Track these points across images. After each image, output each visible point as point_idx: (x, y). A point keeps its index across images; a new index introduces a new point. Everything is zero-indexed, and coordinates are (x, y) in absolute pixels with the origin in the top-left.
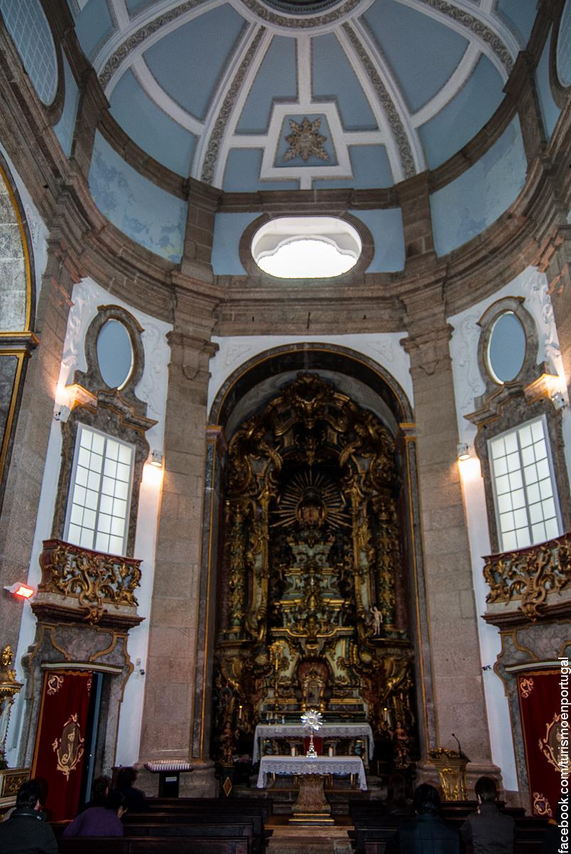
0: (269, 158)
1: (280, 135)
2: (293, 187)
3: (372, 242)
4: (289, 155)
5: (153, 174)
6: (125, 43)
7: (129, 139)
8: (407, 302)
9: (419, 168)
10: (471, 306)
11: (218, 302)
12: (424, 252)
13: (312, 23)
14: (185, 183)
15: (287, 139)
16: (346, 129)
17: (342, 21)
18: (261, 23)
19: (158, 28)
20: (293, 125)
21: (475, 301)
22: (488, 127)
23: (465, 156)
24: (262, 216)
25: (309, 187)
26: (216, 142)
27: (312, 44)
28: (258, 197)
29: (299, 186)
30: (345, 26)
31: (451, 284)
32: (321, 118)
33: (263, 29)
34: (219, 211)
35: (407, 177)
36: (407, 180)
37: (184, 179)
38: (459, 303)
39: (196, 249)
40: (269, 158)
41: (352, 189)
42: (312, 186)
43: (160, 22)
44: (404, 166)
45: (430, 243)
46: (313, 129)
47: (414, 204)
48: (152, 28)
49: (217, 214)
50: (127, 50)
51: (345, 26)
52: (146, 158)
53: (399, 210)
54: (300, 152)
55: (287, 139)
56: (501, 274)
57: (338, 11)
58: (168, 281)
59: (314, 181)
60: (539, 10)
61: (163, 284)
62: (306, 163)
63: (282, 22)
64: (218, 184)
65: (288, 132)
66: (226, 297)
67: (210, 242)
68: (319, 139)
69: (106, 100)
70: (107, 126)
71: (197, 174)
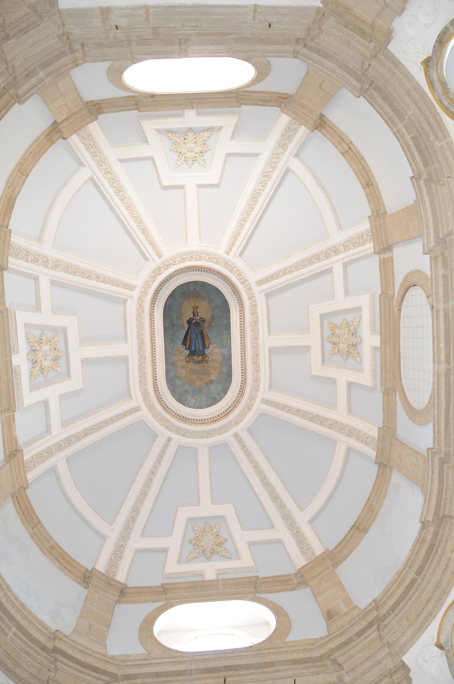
0: (173, 555)
1: (184, 537)
2: (199, 579)
3: (287, 615)
4: (193, 555)
5: (56, 559)
6: (54, 445)
7: (40, 522)
8: (341, 660)
9: (319, 550)
10: (419, 637)
11: (108, 679)
12: (344, 610)
13: (210, 434)
14: (88, 574)
15: (190, 541)
16: (243, 529)
17: (233, 431)
18: (169, 434)
19: (84, 437)
20: (196, 528)
21: (421, 629)
22: (372, 498)
23: (358, 529)
24: (165, 604)
25: (214, 578)
26: (123, 544)
27: (209, 454)
28: (162, 590)
29: (204, 578)
30: (236, 436)
31: (386, 626)
32: (222, 518)
33: (169, 439)
34: (118, 602)
35: (308, 561)
36: (309, 564)
37: (87, 570)
38: (404, 640)
39: (90, 626)
40: (173, 555)
41: (258, 577)
42: (217, 577)
43: (86, 433)
44: (303, 553)
45: (348, 601)
46: (215, 531)
47: (322, 579)
48: (78, 437)
49: (117, 605)
50: (54, 451)
51: (236, 436)
52: (52, 543)
53: (308, 590)
54: (203, 551)
55: (190, 541)
56: (438, 586)
57: (229, 423)
58: (50, 646)
59: (219, 572)
60: (383, 393)
61: (44, 648)
62: (209, 559)
63: (185, 434)
64: (121, 577)
65: (191, 535)
66: (120, 673)
67: (108, 624)
68: (221, 540)
69: (27, 481)
70: (22, 505)
71: (101, 567)
